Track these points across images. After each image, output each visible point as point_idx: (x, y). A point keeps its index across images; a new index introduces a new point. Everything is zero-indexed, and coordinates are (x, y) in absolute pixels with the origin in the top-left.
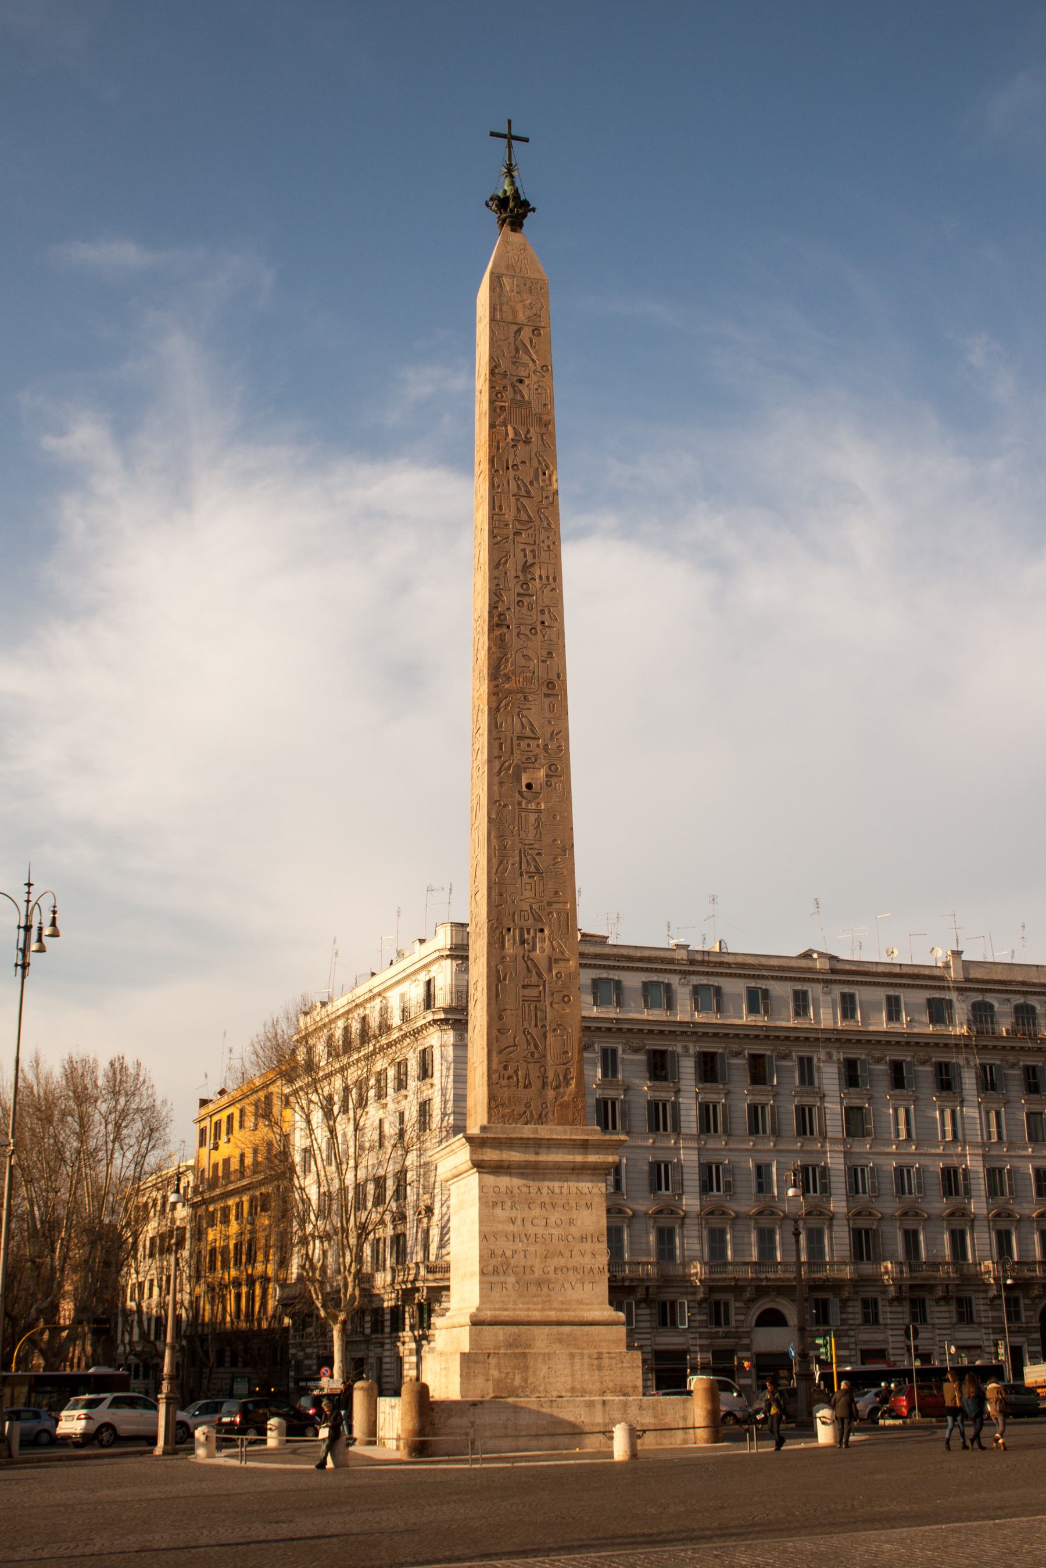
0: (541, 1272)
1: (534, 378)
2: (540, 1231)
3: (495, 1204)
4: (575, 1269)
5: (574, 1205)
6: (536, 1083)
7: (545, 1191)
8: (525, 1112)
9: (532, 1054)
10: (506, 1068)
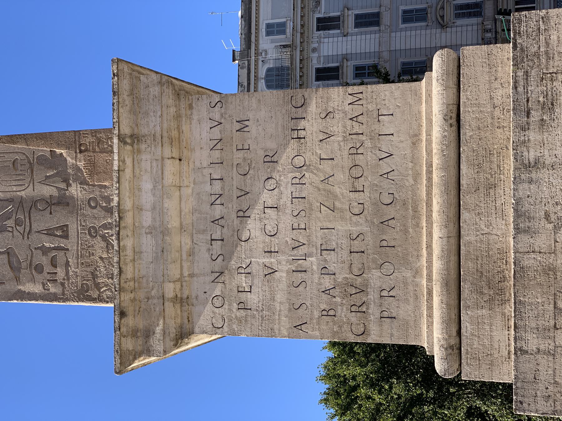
0: (361, 219)
3: (243, 306)
4: (355, 152)
5: (241, 154)
7: (218, 211)
8: (104, 238)
9: (18, 223)
10: (39, 269)
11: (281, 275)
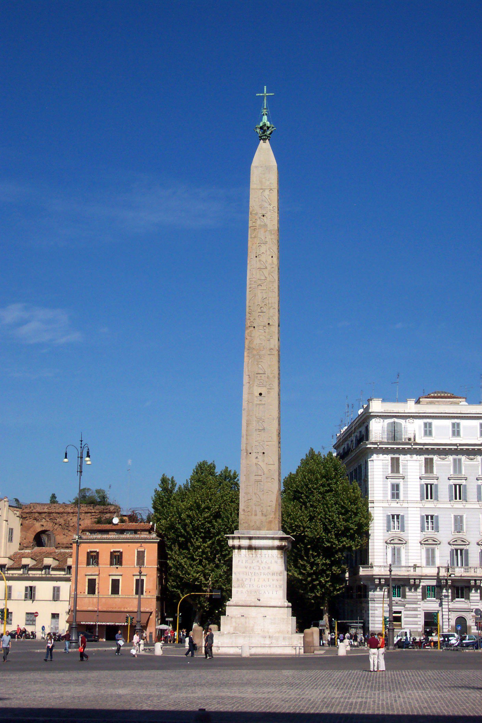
1: (269, 213)
2: (257, 571)
4: (270, 586)
6: (259, 514)
11: (245, 570)
